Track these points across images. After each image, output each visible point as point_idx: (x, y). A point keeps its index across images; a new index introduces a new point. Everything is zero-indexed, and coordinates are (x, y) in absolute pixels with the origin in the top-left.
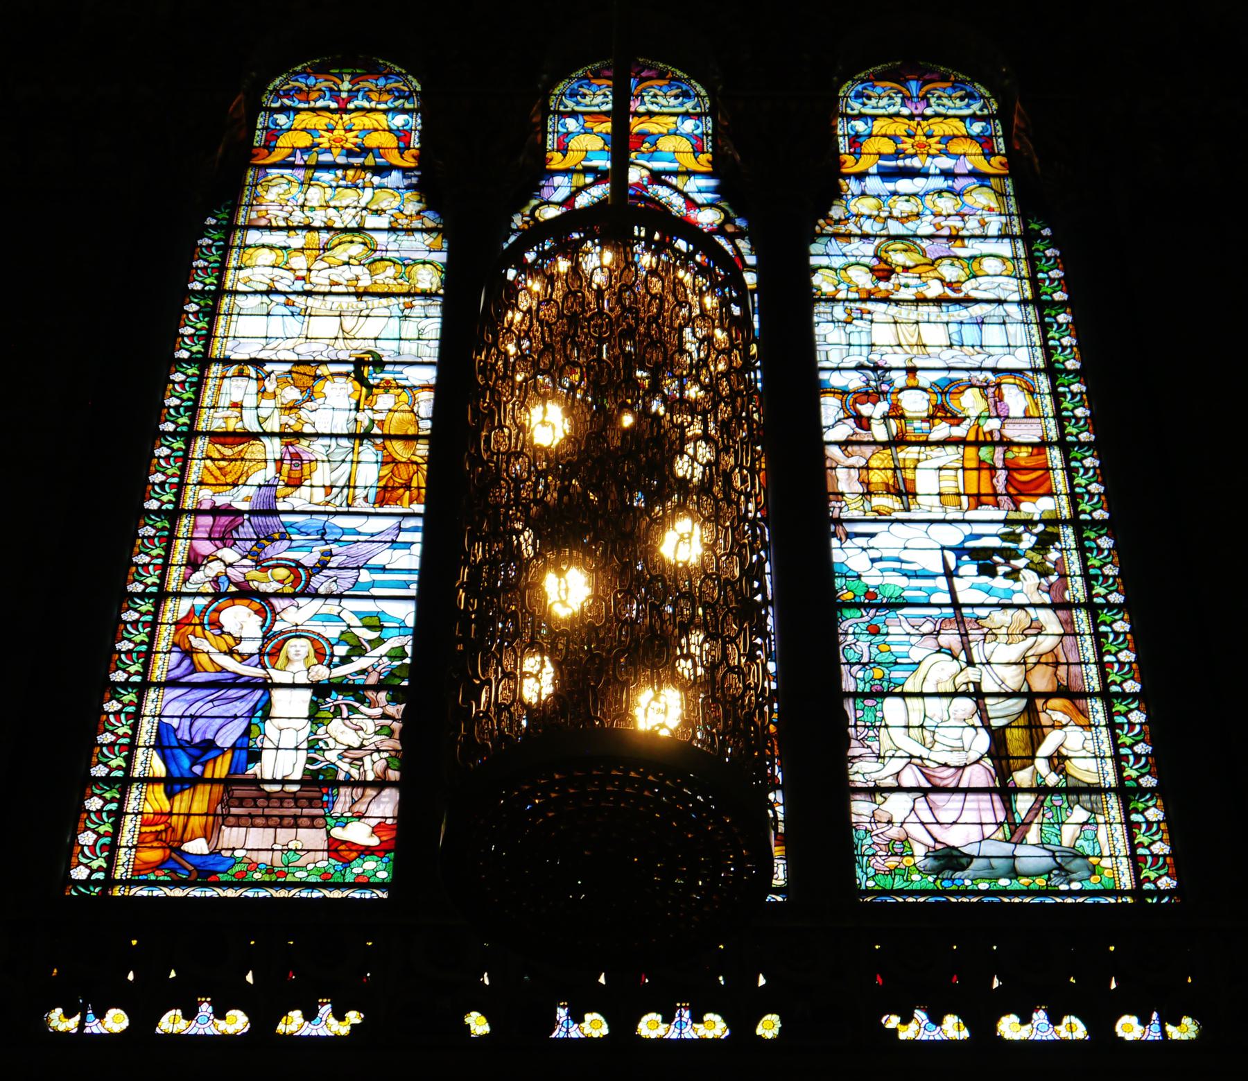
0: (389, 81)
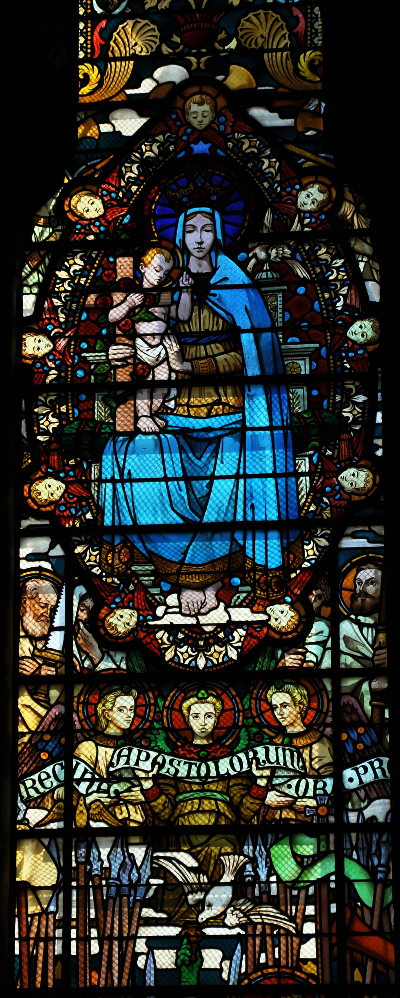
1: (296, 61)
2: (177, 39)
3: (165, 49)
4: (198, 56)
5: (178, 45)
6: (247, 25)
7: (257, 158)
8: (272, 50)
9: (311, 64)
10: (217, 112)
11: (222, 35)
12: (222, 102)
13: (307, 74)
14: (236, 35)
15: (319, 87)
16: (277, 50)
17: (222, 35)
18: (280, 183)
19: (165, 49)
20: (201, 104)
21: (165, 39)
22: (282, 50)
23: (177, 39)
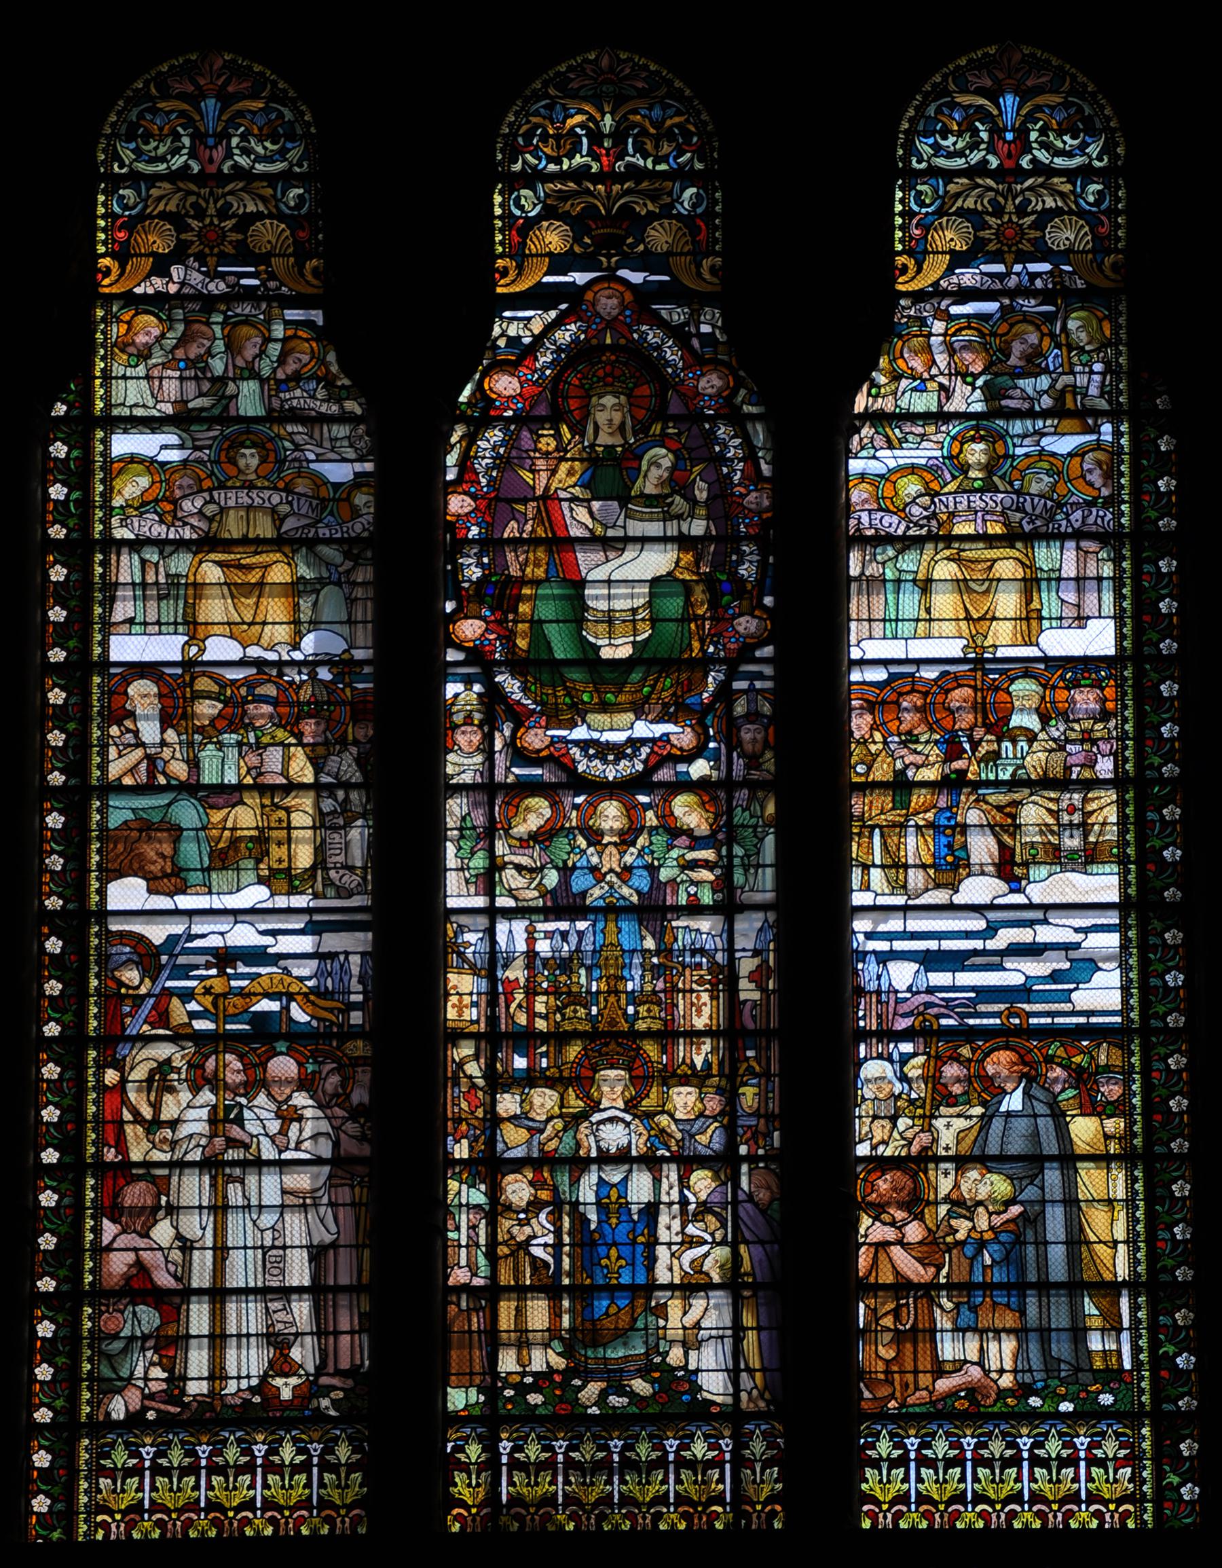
0: (670, 112)
1: (699, 266)
2: (587, 240)
3: (577, 249)
4: (609, 257)
5: (589, 246)
6: (653, 232)
8: (677, 254)
9: (712, 270)
10: (623, 306)
11: (630, 240)
13: (707, 276)
14: (643, 241)
15: (718, 289)
16: (681, 254)
17: (630, 240)
19: (577, 249)
21: (577, 240)
22: (686, 254)
23: (587, 240)
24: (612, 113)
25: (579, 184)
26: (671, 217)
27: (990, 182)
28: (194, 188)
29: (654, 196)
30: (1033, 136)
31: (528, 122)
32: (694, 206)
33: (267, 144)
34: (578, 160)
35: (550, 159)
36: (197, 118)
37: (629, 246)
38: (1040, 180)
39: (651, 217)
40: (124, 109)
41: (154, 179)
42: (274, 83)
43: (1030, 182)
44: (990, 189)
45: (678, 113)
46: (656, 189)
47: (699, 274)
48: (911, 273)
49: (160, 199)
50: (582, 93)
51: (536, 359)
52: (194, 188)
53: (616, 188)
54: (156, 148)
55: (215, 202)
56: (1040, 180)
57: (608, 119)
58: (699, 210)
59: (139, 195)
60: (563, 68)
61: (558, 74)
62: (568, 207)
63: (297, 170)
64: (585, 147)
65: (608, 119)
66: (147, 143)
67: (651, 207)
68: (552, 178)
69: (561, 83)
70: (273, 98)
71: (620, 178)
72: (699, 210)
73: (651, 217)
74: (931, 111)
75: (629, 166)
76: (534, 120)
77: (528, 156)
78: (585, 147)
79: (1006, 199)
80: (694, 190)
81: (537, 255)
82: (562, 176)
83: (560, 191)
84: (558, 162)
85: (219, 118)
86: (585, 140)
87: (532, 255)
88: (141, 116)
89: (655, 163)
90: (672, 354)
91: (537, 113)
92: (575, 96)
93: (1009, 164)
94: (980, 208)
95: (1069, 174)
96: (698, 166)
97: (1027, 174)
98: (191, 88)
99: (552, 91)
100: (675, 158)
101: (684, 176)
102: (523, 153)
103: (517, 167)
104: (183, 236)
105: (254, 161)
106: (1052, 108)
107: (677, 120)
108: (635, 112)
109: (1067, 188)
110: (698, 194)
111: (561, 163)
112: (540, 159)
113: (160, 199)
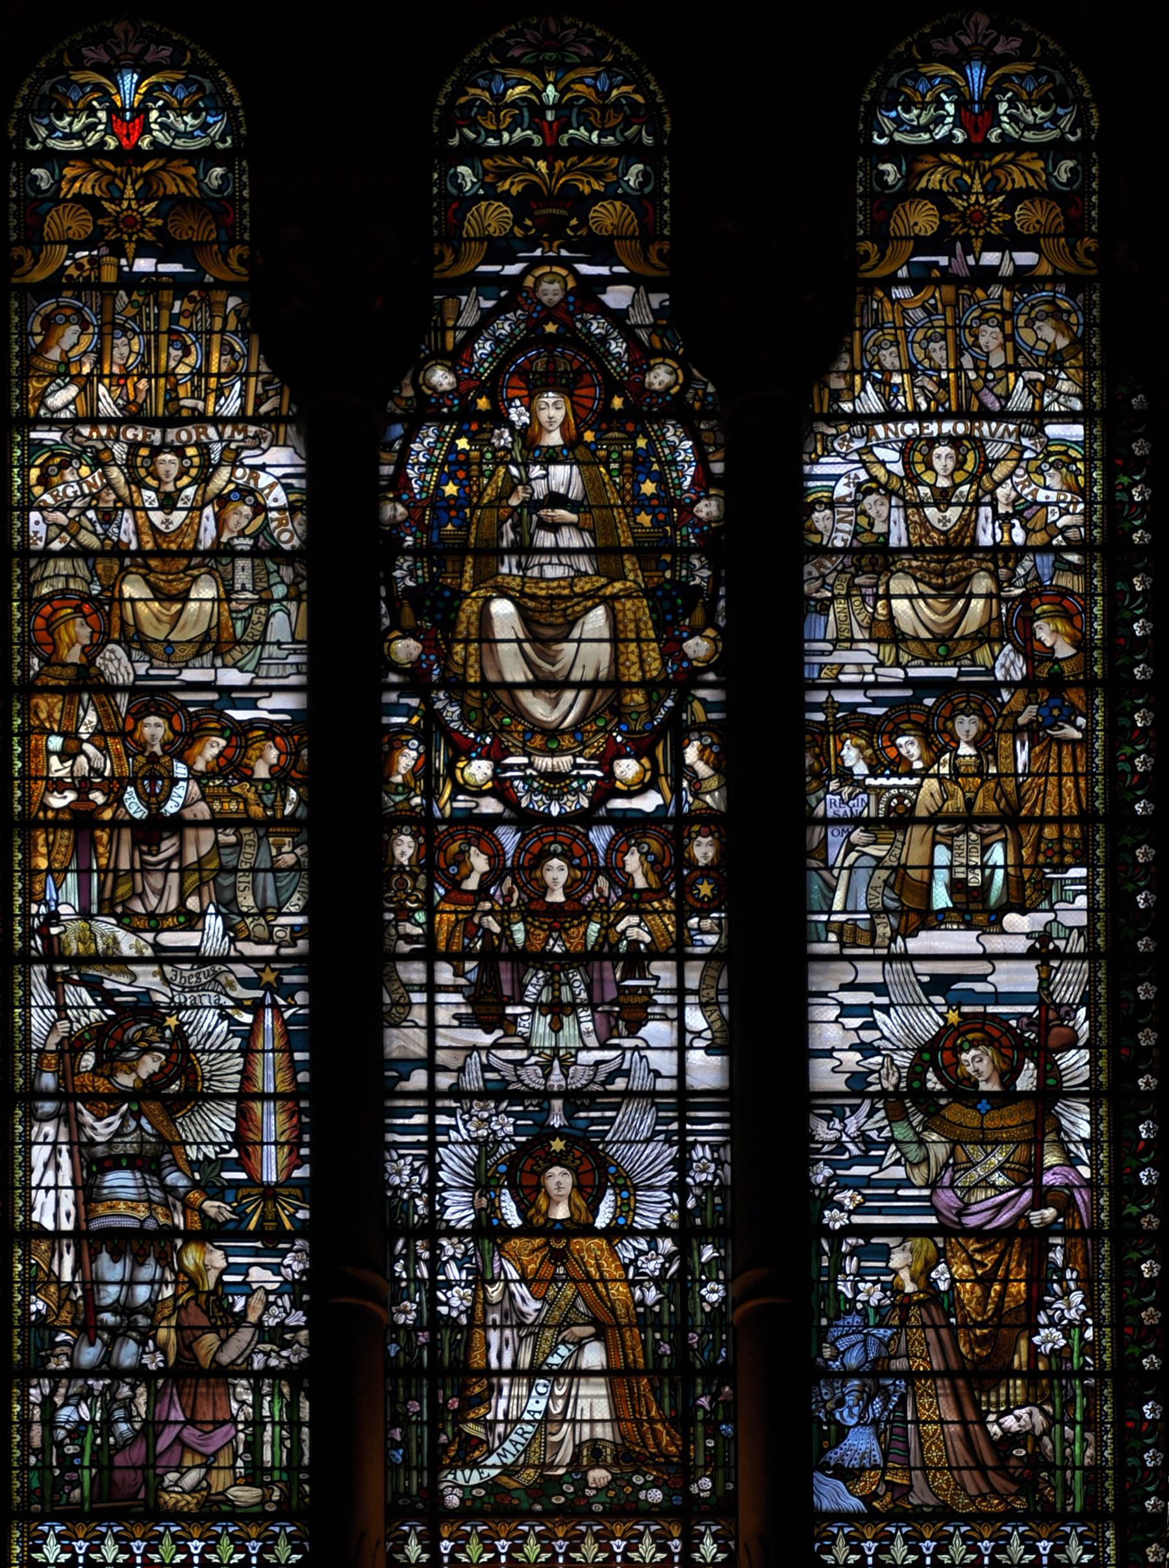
2: (528, 222)
3: (518, 232)
5: (527, 229)
7: (604, 340)
11: (574, 222)
12: (571, 284)
17: (574, 222)
18: (628, 363)
19: (518, 232)
20: (551, 282)
21: (518, 221)
23: (528, 222)
24: (555, 84)
25: (519, 160)
26: (617, 197)
27: (956, 159)
28: (111, 167)
29: (598, 174)
30: (1003, 107)
31: (467, 94)
32: (642, 185)
33: (188, 119)
34: (519, 134)
35: (490, 134)
36: (113, 91)
37: (574, 228)
38: (1010, 156)
39: (596, 197)
40: (36, 81)
41: (67, 157)
42: (194, 53)
43: (997, 159)
44: (955, 166)
45: (625, 82)
46: (602, 167)
47: (646, 259)
48: (872, 262)
49: (74, 180)
50: (524, 60)
51: (474, 351)
52: (111, 167)
53: (559, 164)
54: (71, 124)
55: (133, 184)
56: (1010, 156)
57: (551, 90)
58: (647, 190)
59: (53, 175)
60: (502, 35)
61: (498, 41)
62: (506, 186)
63: (220, 146)
64: (526, 119)
65: (551, 90)
66: (61, 118)
67: (596, 187)
68: (491, 152)
69: (500, 49)
70: (191, 69)
71: (564, 154)
72: (647, 190)
73: (596, 197)
74: (894, 81)
75: (572, 140)
76: (472, 91)
77: (466, 131)
78: (526, 119)
79: (972, 178)
80: (641, 167)
81: (475, 239)
82: (503, 150)
83: (499, 167)
84: (499, 136)
85: (136, 92)
86: (526, 114)
87: (469, 239)
88: (53, 89)
89: (599, 136)
90: (617, 347)
91: (477, 86)
92: (515, 63)
93: (977, 139)
94: (945, 188)
95: (1041, 149)
96: (648, 140)
97: (995, 149)
98: (106, 58)
99: (493, 60)
100: (622, 132)
101: (630, 151)
102: (460, 127)
103: (455, 142)
104: (100, 222)
105: (174, 138)
106: (1021, 77)
107: (624, 89)
108: (581, 80)
109: (1038, 165)
110: (644, 173)
111: (500, 137)
112: (478, 134)
113: (74, 180)
